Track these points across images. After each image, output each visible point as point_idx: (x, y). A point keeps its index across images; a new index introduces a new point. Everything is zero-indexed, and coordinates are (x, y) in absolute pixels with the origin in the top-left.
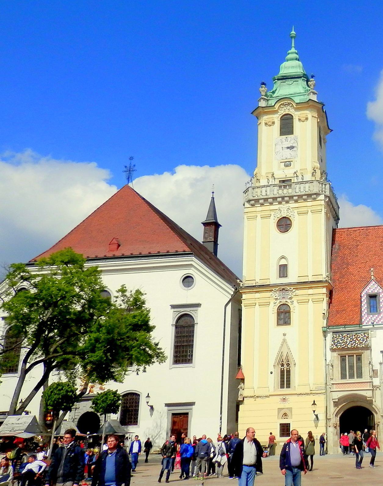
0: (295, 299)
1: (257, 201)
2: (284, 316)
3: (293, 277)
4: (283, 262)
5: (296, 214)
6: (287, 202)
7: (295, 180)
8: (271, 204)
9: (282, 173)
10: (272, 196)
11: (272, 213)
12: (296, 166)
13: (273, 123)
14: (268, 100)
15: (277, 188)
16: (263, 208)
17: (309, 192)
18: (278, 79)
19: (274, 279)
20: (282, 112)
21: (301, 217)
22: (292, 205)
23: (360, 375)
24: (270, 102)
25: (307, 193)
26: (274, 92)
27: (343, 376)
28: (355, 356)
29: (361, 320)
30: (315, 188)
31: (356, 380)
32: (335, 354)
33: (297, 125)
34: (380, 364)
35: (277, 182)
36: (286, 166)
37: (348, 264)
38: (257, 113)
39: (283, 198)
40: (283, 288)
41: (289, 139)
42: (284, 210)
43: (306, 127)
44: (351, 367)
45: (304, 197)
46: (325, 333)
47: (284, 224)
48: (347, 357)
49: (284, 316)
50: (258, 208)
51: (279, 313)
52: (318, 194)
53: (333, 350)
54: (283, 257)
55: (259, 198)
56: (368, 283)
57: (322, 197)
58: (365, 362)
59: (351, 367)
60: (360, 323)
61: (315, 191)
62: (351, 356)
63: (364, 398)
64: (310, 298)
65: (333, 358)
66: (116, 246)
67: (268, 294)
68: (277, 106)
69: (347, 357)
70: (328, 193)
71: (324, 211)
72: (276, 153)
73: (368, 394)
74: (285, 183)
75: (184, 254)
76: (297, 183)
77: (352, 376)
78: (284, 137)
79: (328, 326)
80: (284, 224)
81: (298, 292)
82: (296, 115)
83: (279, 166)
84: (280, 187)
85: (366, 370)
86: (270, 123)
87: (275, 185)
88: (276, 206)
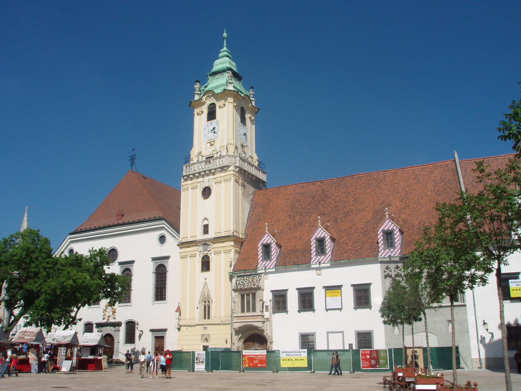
0: (212, 252)
1: (188, 176)
2: (206, 265)
3: (211, 235)
4: (206, 222)
5: (214, 184)
6: (208, 175)
7: (215, 156)
8: (198, 178)
9: (206, 153)
10: (198, 171)
11: (199, 185)
12: (217, 146)
13: (202, 112)
14: (200, 94)
15: (204, 164)
16: (194, 181)
17: (222, 165)
18: (210, 76)
19: (200, 236)
20: (208, 102)
21: (218, 185)
22: (211, 177)
23: (254, 310)
24: (202, 95)
25: (220, 166)
26: (206, 87)
27: (243, 311)
28: (251, 295)
29: (257, 266)
30: (225, 162)
31: (251, 314)
32: (237, 294)
33: (218, 112)
34: (270, 301)
35: (204, 159)
36: (211, 145)
37: (259, 220)
38: (192, 105)
39: (205, 172)
40: (205, 243)
41: (213, 123)
42: (206, 181)
43: (227, 112)
44: (248, 303)
45: (213, 171)
46: (231, 278)
47: (207, 192)
48: (245, 295)
49: (206, 265)
50: (189, 182)
51: (203, 263)
52: (228, 167)
53: (235, 290)
54: (206, 219)
55: (190, 173)
56: (264, 234)
57: (232, 168)
58: (257, 299)
59: (248, 303)
60: (256, 268)
61: (227, 164)
62: (248, 295)
63: (256, 328)
64: (222, 249)
65: (237, 297)
66: (120, 216)
67: (195, 248)
68: (204, 98)
69: (245, 295)
70: (238, 165)
71: (233, 179)
72: (205, 136)
73: (259, 325)
74: (209, 159)
75: (160, 219)
76: (217, 158)
77: (248, 311)
78: (210, 122)
79: (234, 271)
80: (207, 192)
81: (215, 246)
82: (218, 104)
83: (206, 146)
84: (206, 162)
85: (258, 305)
86: (200, 113)
87: (201, 162)
88: (200, 179)
